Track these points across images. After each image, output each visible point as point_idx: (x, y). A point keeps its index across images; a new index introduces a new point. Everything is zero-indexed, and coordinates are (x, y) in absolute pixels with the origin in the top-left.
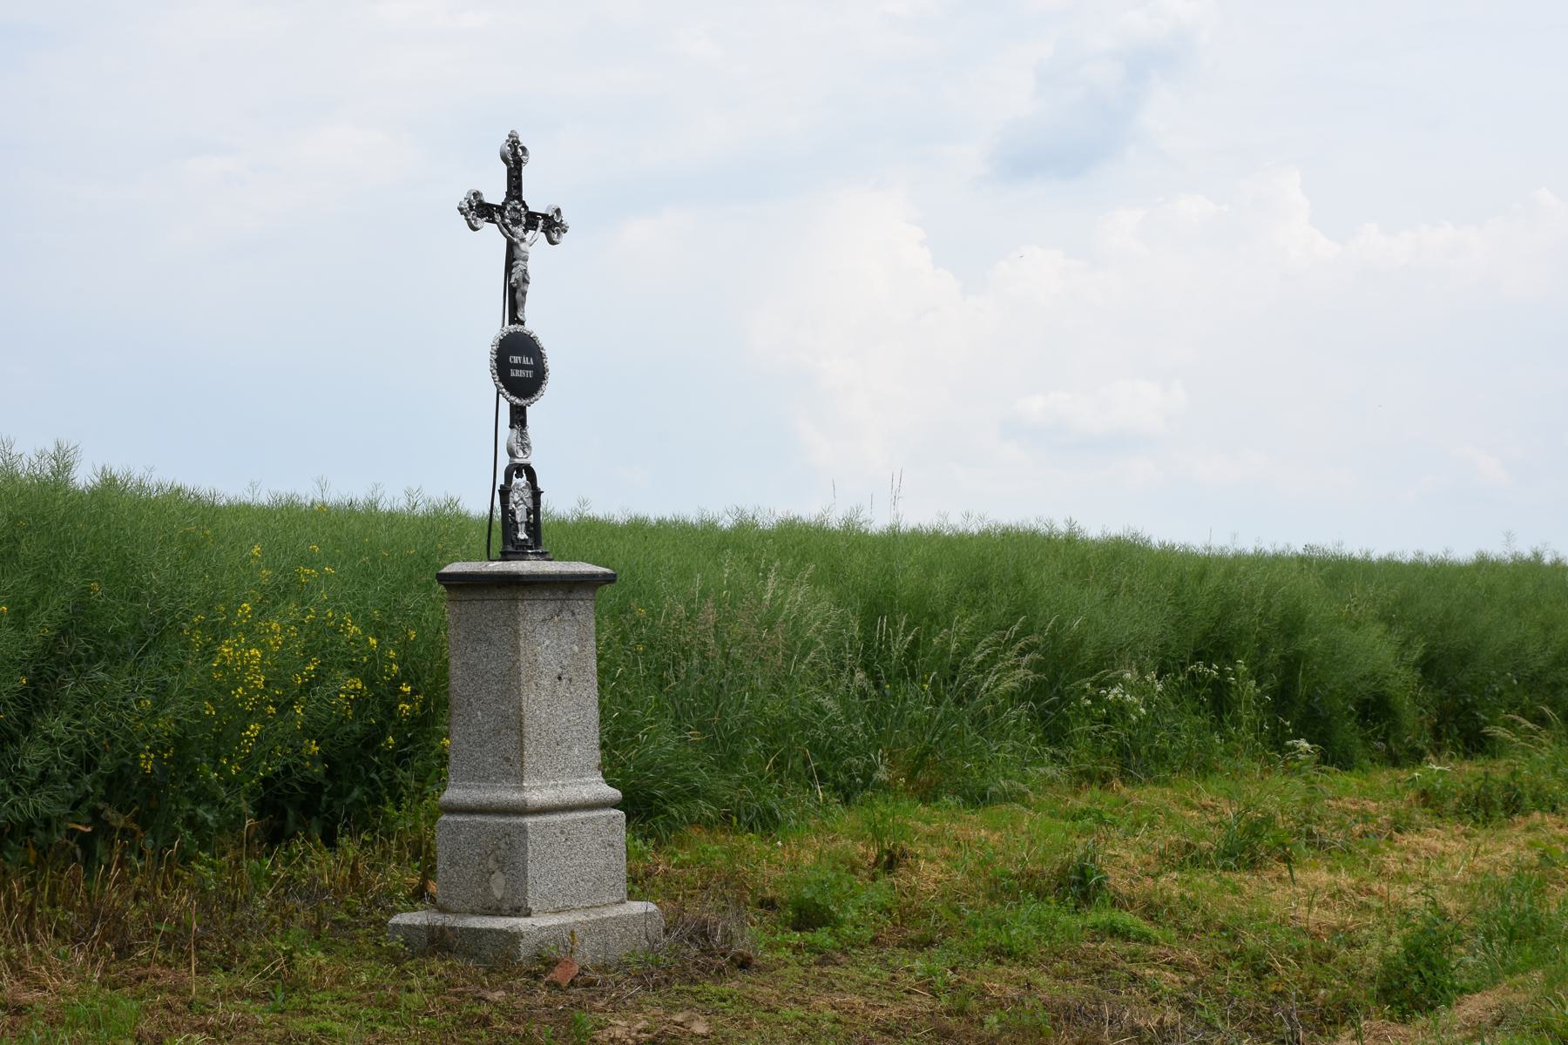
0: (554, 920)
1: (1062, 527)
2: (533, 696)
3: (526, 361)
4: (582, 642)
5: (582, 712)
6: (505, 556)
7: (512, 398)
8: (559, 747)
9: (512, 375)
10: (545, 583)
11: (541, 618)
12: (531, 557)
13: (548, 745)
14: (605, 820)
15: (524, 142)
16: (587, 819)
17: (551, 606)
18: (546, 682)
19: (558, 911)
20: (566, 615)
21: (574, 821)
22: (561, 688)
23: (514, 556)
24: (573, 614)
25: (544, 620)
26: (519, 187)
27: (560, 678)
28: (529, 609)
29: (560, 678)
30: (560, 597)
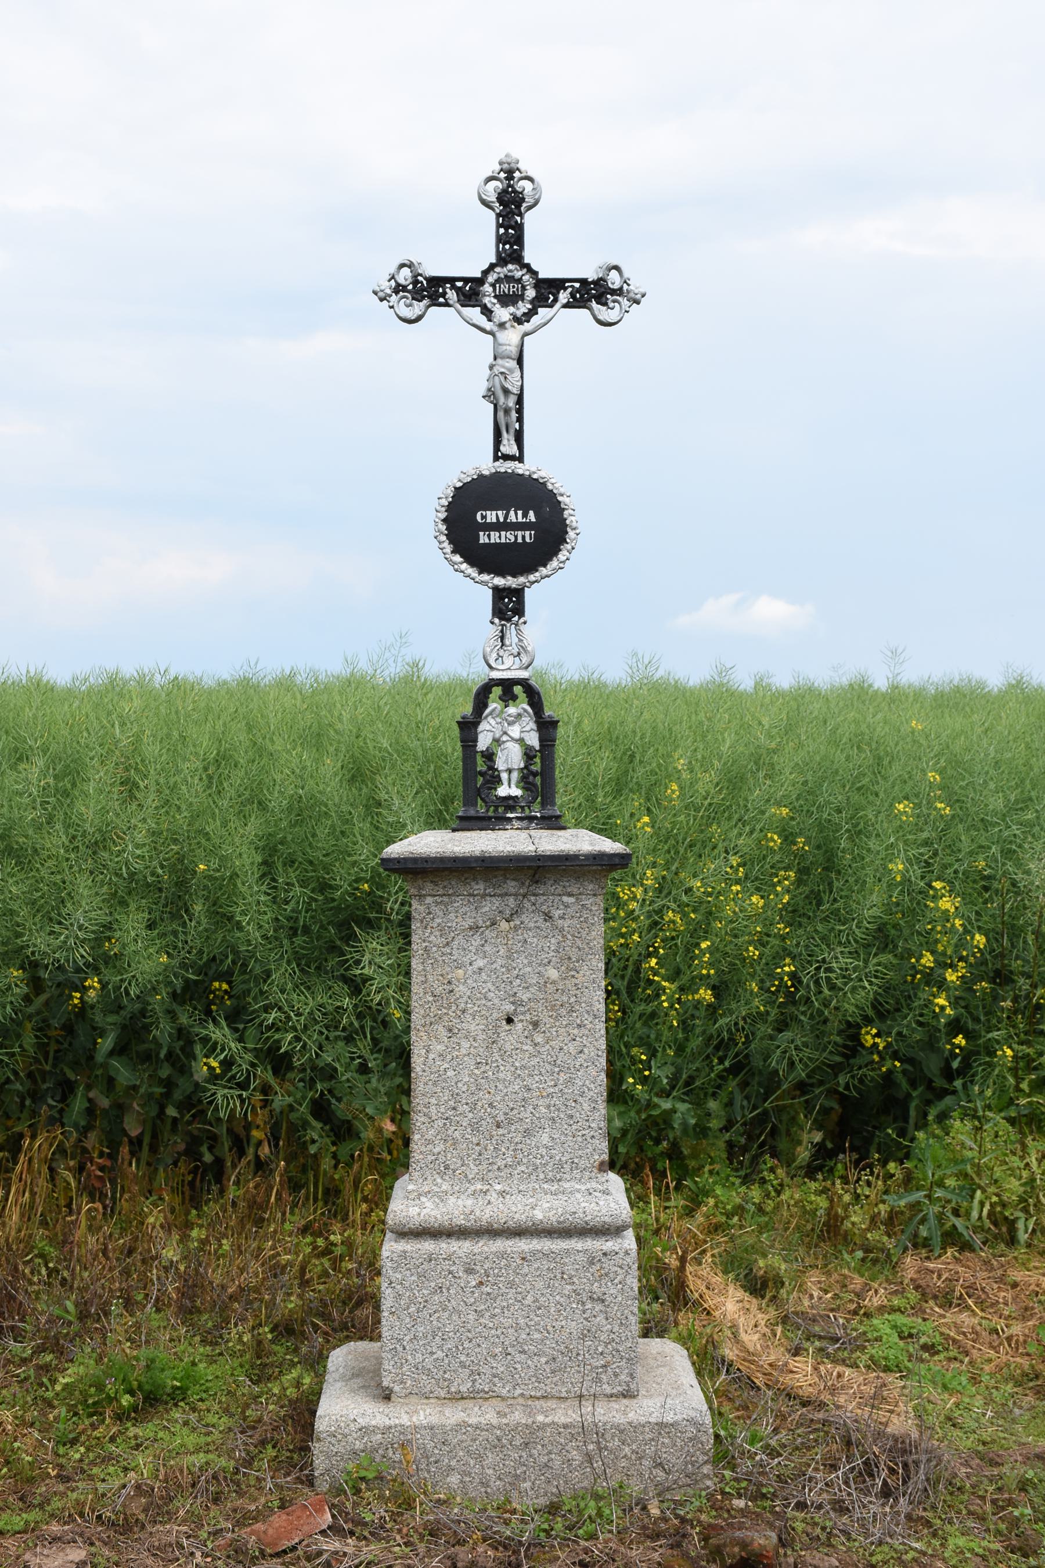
0: (453, 1415)
1: (392, 670)
2: (440, 1048)
3: (515, 516)
4: (569, 964)
5: (562, 1077)
6: (468, 823)
7: (485, 577)
8: (501, 1131)
9: (481, 534)
10: (451, 870)
11: (470, 922)
12: (516, 824)
13: (475, 1127)
14: (580, 1257)
15: (526, 166)
16: (533, 1253)
17: (489, 906)
18: (474, 1026)
19: (458, 1397)
20: (530, 919)
21: (503, 1255)
22: (511, 1037)
23: (480, 824)
24: (548, 917)
25: (475, 928)
26: (519, 239)
27: (510, 1021)
28: (436, 910)
29: (510, 1021)
30: (512, 890)
